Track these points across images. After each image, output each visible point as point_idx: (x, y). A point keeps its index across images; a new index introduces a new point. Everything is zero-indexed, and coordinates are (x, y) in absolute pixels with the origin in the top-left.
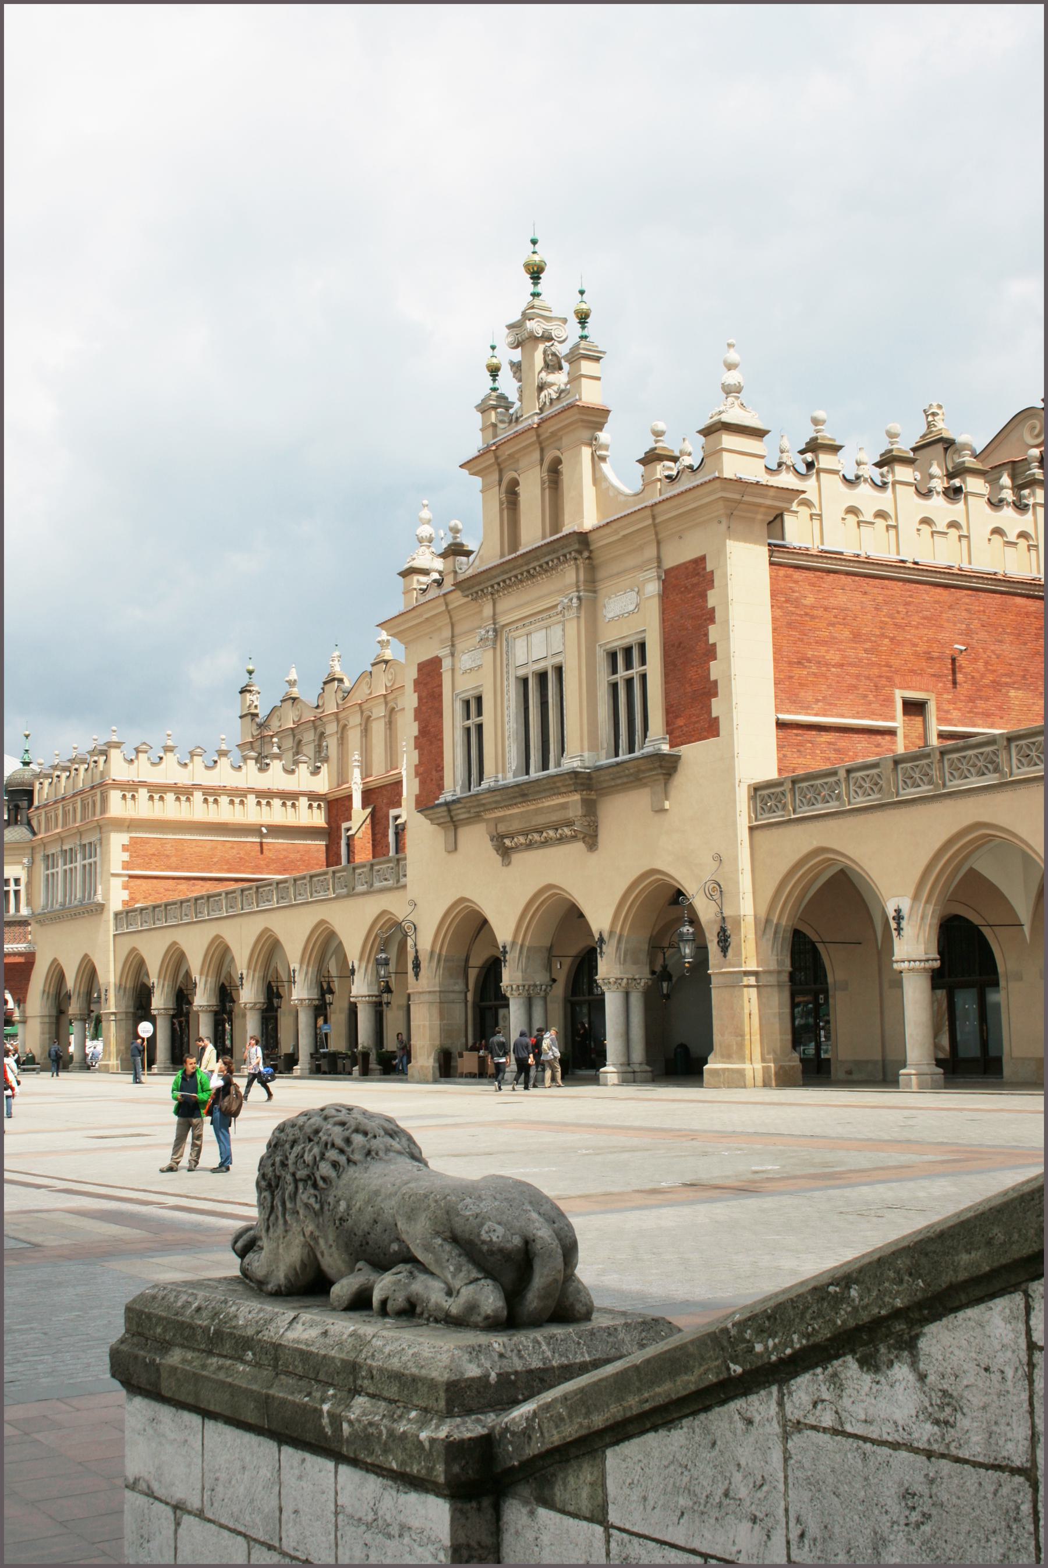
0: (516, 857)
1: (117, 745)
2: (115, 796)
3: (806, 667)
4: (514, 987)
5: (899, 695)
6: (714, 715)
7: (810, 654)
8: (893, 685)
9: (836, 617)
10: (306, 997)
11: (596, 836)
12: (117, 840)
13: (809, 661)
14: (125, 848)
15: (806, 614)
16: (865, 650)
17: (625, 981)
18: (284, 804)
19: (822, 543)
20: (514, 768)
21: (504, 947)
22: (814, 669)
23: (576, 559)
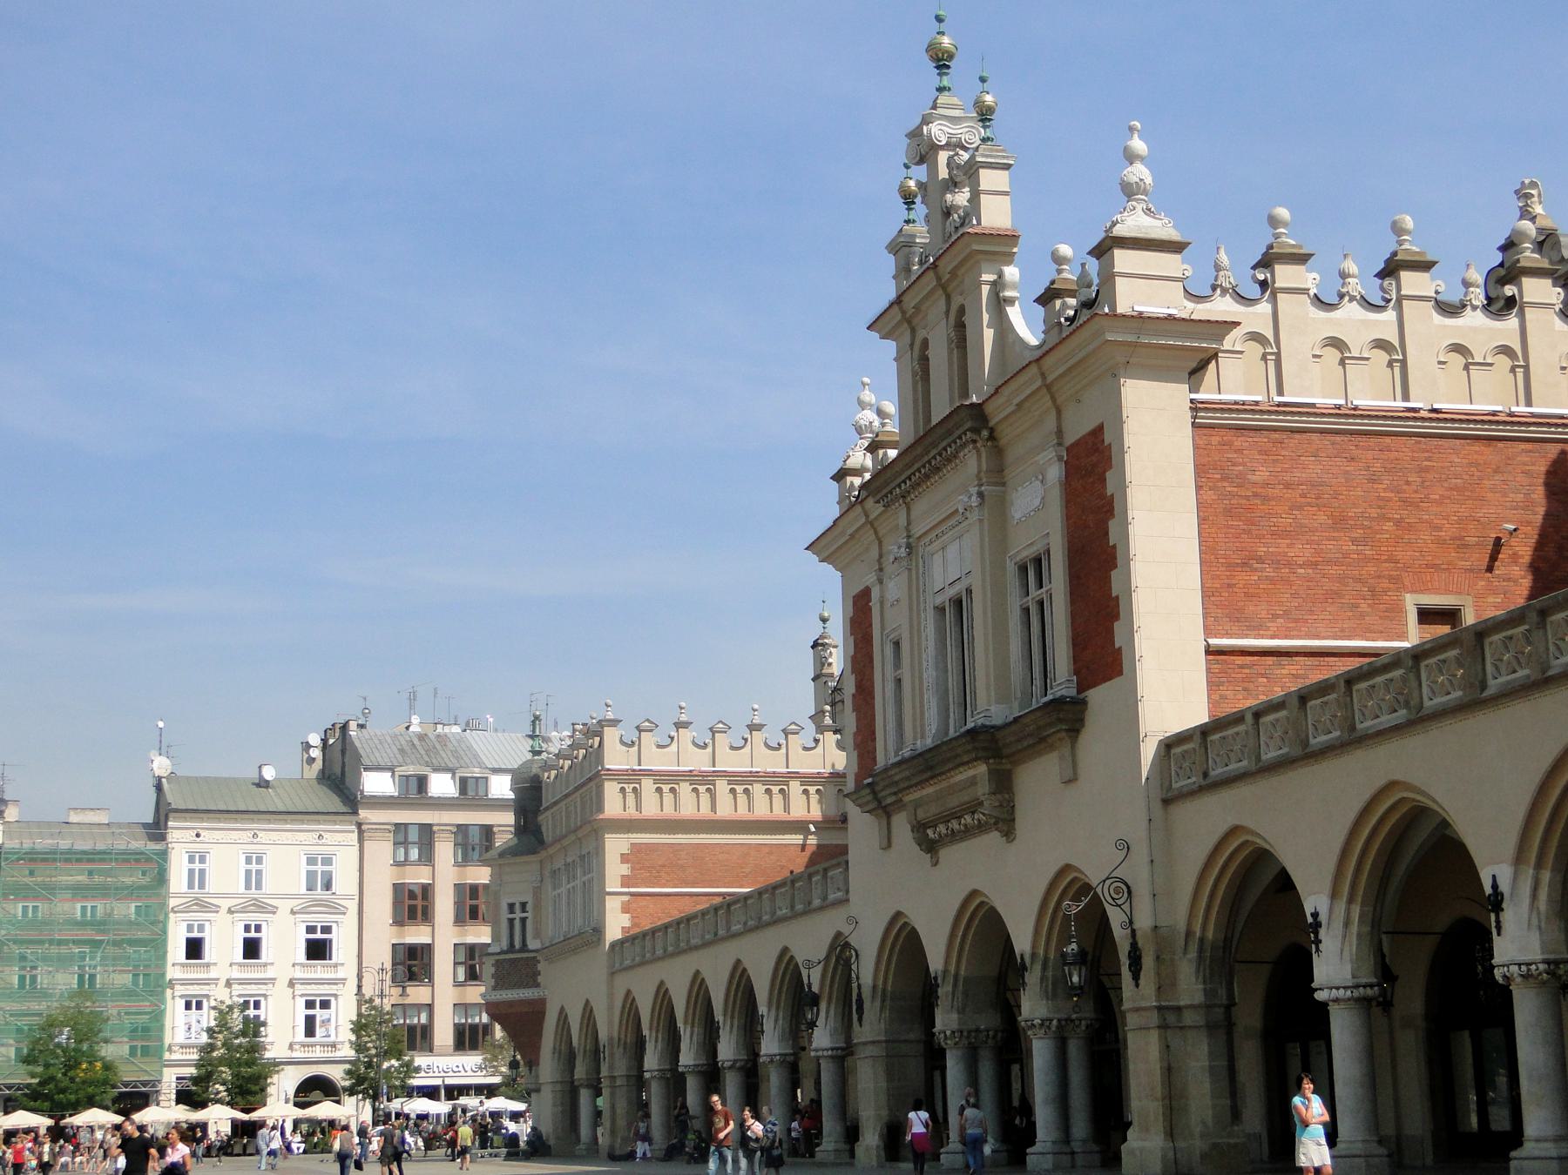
0: (945, 853)
1: (614, 723)
2: (611, 790)
3: (1256, 570)
4: (948, 1033)
5: (1411, 603)
6: (1117, 646)
7: (1262, 550)
8: (1398, 584)
9: (1303, 496)
10: (776, 1051)
11: (1014, 820)
12: (615, 846)
13: (1260, 560)
14: (624, 858)
15: (1256, 495)
16: (1354, 541)
17: (1055, 1022)
18: (695, 790)
19: (1280, 392)
20: (934, 731)
21: (936, 978)
22: (1269, 572)
23: (974, 442)
